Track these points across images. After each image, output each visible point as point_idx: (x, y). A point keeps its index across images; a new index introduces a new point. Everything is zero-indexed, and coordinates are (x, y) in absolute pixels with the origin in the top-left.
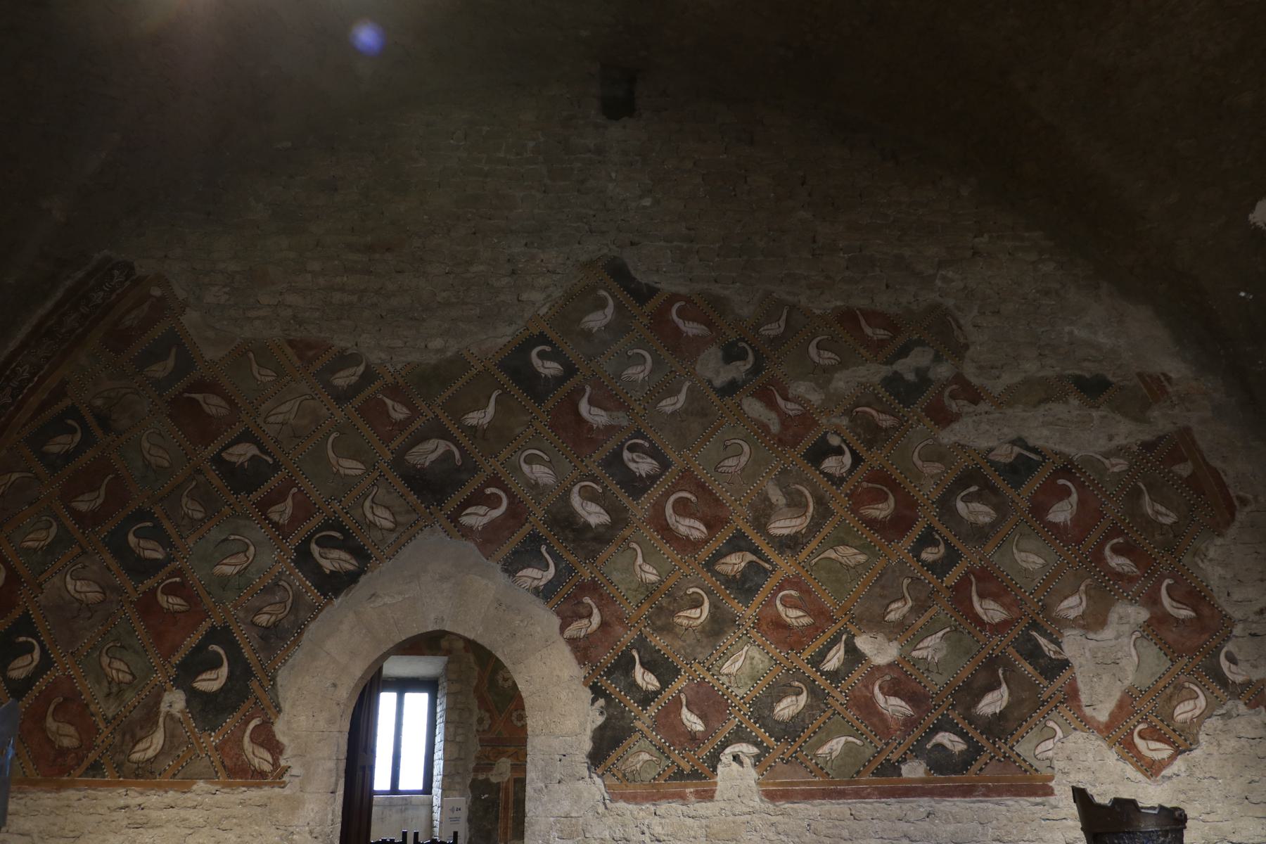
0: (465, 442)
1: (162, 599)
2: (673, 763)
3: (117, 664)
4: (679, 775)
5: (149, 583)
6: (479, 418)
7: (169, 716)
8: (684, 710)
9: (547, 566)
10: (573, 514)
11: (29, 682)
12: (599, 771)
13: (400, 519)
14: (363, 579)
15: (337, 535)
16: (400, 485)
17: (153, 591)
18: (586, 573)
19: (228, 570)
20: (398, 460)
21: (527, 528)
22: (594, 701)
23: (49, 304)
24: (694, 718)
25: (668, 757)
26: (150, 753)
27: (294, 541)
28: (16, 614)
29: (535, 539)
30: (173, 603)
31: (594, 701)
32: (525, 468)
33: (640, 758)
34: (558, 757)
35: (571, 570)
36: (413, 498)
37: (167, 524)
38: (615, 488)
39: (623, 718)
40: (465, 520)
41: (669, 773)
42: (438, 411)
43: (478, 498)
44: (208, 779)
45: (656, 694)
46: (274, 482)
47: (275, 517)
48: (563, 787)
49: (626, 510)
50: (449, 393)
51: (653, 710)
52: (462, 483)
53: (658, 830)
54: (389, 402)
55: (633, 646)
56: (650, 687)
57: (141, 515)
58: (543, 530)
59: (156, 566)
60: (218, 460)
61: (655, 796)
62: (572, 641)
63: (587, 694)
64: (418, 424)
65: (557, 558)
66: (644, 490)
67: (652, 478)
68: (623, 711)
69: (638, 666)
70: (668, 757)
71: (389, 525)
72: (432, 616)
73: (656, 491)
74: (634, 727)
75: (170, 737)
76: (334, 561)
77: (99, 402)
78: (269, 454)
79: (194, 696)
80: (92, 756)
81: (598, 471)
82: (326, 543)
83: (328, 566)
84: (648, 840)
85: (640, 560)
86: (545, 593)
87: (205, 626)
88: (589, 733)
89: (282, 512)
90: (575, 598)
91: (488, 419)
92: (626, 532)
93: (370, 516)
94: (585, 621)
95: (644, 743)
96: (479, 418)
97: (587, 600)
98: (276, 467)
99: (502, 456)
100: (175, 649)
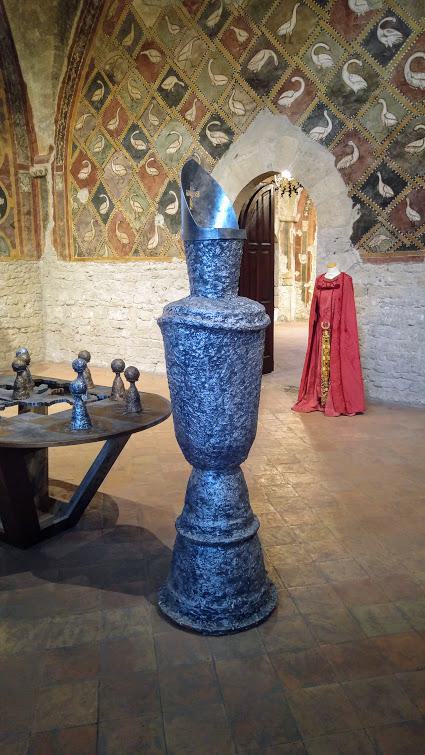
0: (279, 48)
1: (148, 170)
3: (137, 204)
4: (403, 248)
5: (142, 162)
6: (286, 28)
7: (159, 227)
8: (408, 208)
9: (328, 124)
10: (343, 85)
11: (107, 215)
13: (248, 108)
14: (231, 147)
15: (217, 123)
16: (245, 85)
17: (143, 166)
18: (350, 125)
19: (172, 150)
20: (244, 71)
21: (316, 100)
22: (354, 205)
23: (79, 13)
24: (414, 213)
26: (155, 245)
27: (199, 130)
28: (97, 185)
29: (321, 107)
30: (152, 171)
31: (354, 205)
32: (314, 58)
33: (380, 238)
35: (342, 124)
36: (253, 93)
37: (145, 130)
38: (371, 60)
40: (281, 102)
42: (263, 29)
43: (290, 85)
44: (177, 256)
45: (393, 198)
46: (186, 97)
47: (188, 118)
49: (377, 75)
50: (271, 11)
51: (389, 209)
52: (278, 78)
54: (236, 30)
55: (378, 170)
56: (388, 195)
57: (134, 127)
58: (325, 101)
59: (144, 153)
60: (160, 89)
61: (386, 259)
62: (341, 170)
63: (351, 202)
64: (254, 41)
65: (333, 117)
66: (390, 58)
67: (397, 47)
68: (371, 210)
69: (381, 182)
70: (397, 238)
71: (243, 112)
72: (266, 164)
73: (399, 56)
75: (160, 236)
76: (217, 138)
77: (107, 67)
78: (182, 80)
79: (167, 216)
80: (134, 247)
81: (359, 49)
82: (213, 128)
83: (215, 142)
85: (385, 111)
86: (326, 142)
87: (166, 182)
88: (351, 225)
89: (191, 115)
90: (343, 143)
91: (292, 27)
92: (377, 92)
93: (232, 108)
94: (350, 157)
95: (383, 229)
96: (286, 28)
97: (351, 143)
98: (186, 87)
99: (300, 54)
100: (156, 195)
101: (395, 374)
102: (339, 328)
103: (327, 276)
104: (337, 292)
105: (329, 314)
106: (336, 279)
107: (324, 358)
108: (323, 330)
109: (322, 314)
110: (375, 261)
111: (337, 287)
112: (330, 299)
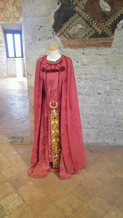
2: (93, 29)
4: (96, 35)
12: (58, 34)
24: (106, 4)
25: (91, 26)
33: (77, 27)
34: (38, 28)
39: (69, 5)
41: (91, 34)
48: (41, 42)
53: (85, 60)
70: (91, 26)
74: (75, 11)
84: (80, 65)
88: (53, 14)
95: (80, 19)
101: (89, 126)
102: (66, 107)
103: (49, 59)
104: (63, 74)
105: (56, 95)
106: (60, 61)
107: (53, 132)
108: (51, 109)
109: (48, 94)
110: (73, 47)
111: (62, 69)
112: (57, 82)
